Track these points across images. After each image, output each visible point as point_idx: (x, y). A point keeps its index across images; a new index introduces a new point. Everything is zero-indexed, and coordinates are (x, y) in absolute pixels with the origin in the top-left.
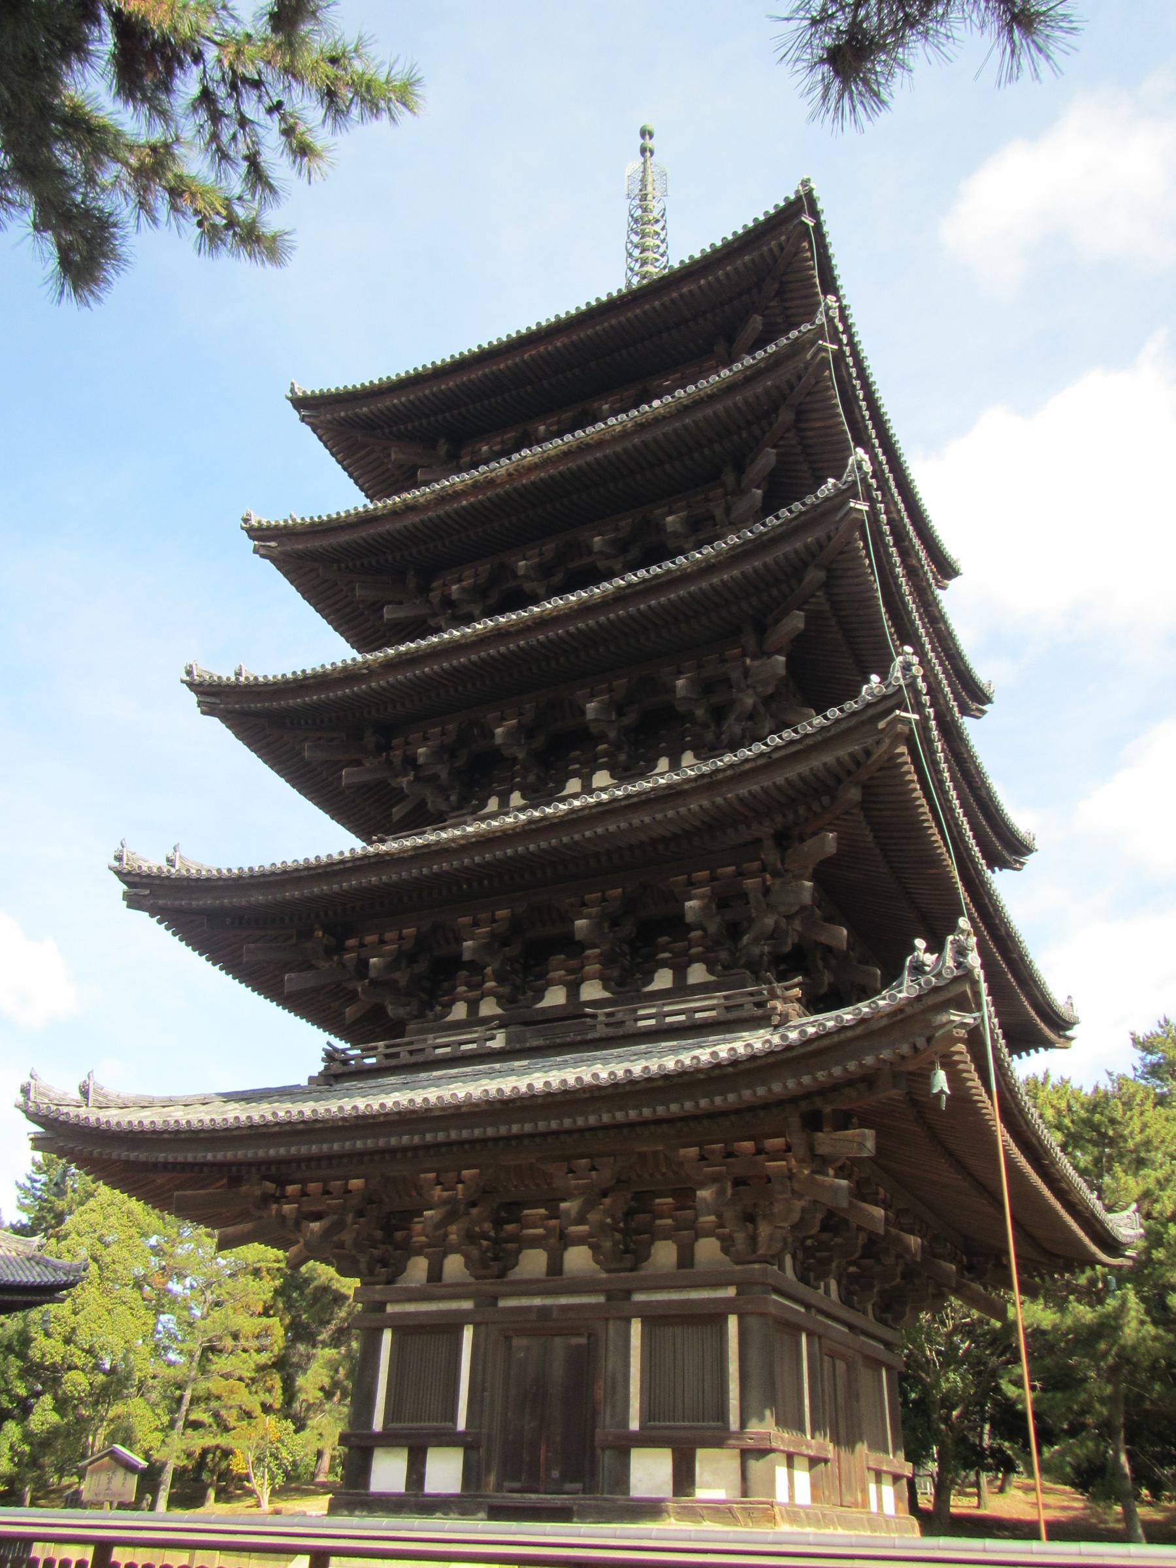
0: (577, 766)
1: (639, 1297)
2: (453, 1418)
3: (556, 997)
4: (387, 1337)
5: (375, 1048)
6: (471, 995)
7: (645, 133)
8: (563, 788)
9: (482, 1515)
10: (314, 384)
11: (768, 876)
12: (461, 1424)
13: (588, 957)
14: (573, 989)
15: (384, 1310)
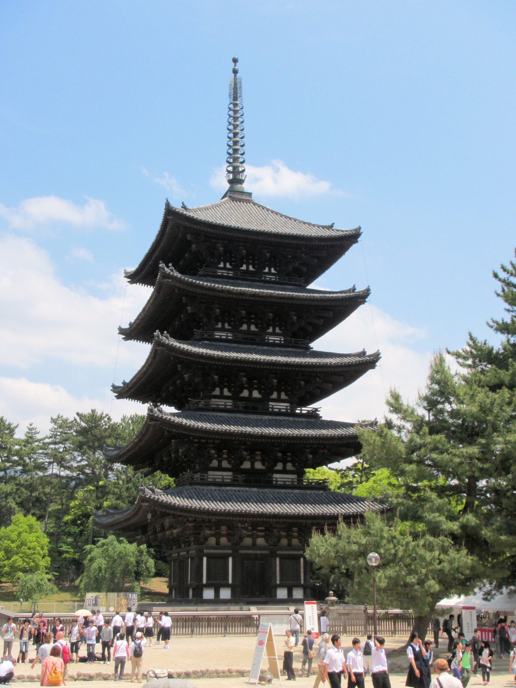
0: (247, 386)
1: (279, 552)
2: (228, 580)
3: (247, 465)
4: (205, 559)
5: (204, 476)
6: (220, 459)
7: (235, 61)
8: (242, 392)
9: (241, 604)
10: (177, 206)
11: (326, 451)
12: (230, 582)
13: (257, 454)
14: (253, 464)
15: (203, 551)
